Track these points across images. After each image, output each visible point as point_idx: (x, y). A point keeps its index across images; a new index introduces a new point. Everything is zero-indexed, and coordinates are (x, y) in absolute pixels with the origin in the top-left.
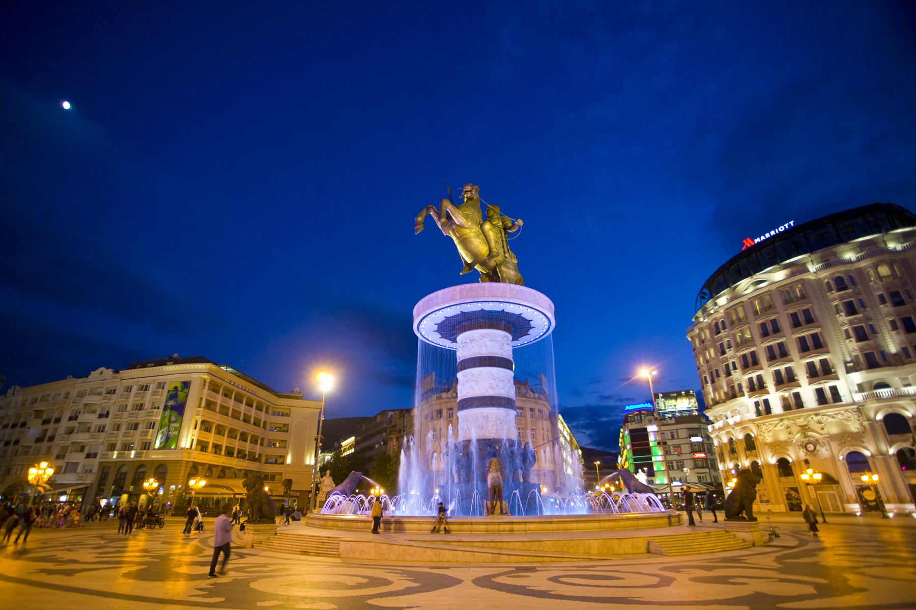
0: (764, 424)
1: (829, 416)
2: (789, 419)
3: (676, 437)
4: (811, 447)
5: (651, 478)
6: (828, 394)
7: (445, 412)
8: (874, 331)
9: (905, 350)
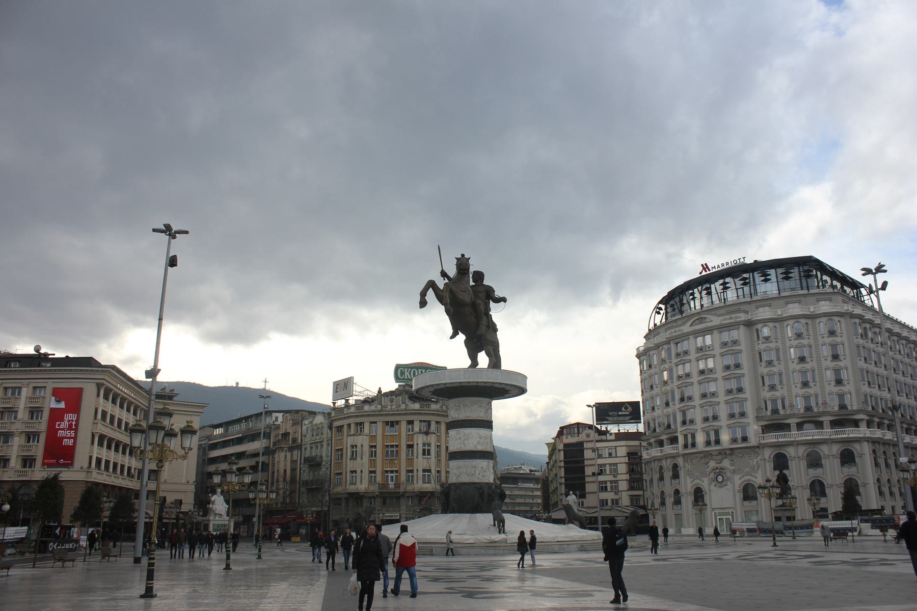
3: (614, 455)
5: (581, 500)
7: (367, 426)
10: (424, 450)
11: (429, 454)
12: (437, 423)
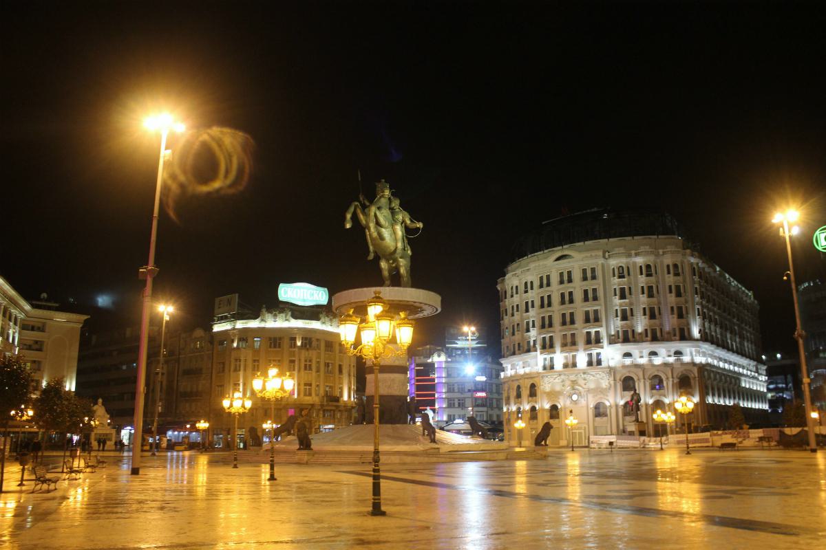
0: (547, 377)
1: (591, 375)
2: (565, 375)
4: (575, 397)
6: (594, 359)
8: (632, 315)
9: (646, 330)
10: (306, 365)
11: (310, 369)
12: (318, 340)
